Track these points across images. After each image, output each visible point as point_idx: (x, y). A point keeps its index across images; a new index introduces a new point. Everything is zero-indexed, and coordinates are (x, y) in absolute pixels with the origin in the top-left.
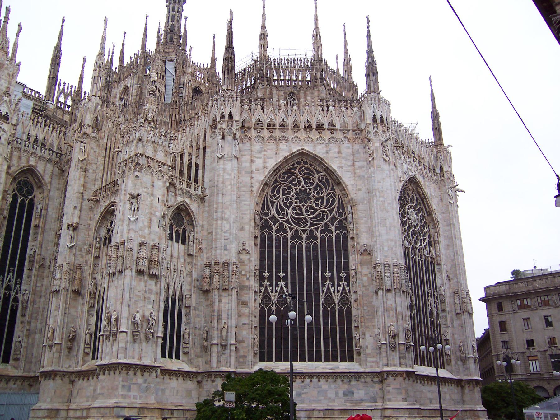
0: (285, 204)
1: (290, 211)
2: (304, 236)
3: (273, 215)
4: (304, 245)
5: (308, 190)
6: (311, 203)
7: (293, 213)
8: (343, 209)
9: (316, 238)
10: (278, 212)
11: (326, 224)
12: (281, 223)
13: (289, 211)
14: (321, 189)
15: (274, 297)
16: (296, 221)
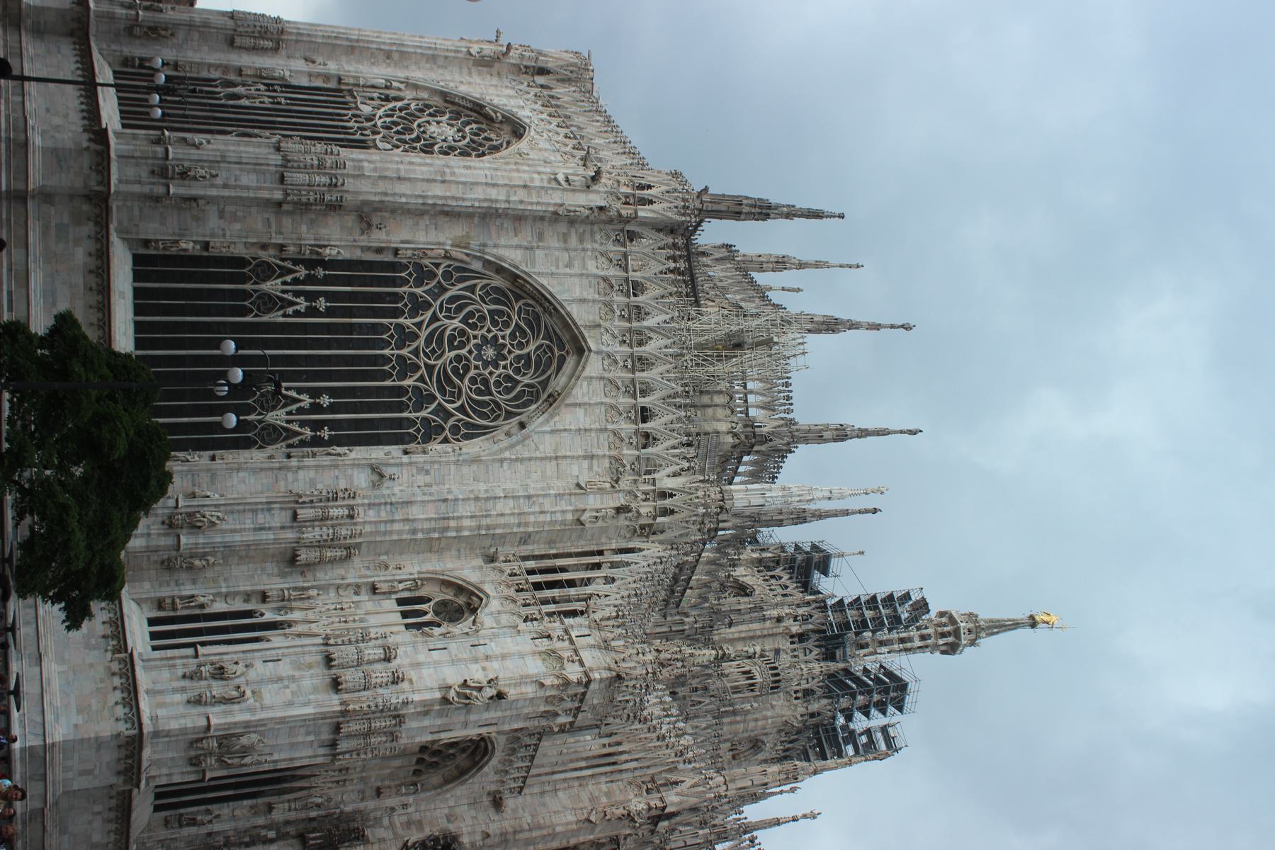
0: (471, 315)
1: (456, 323)
2: (405, 352)
3: (447, 290)
4: (387, 352)
5: (502, 363)
6: (477, 367)
7: (454, 330)
8: (468, 437)
9: (402, 377)
10: (453, 299)
11: (435, 398)
12: (431, 305)
13: (455, 321)
14: (508, 390)
15: (272, 286)
16: (436, 338)
